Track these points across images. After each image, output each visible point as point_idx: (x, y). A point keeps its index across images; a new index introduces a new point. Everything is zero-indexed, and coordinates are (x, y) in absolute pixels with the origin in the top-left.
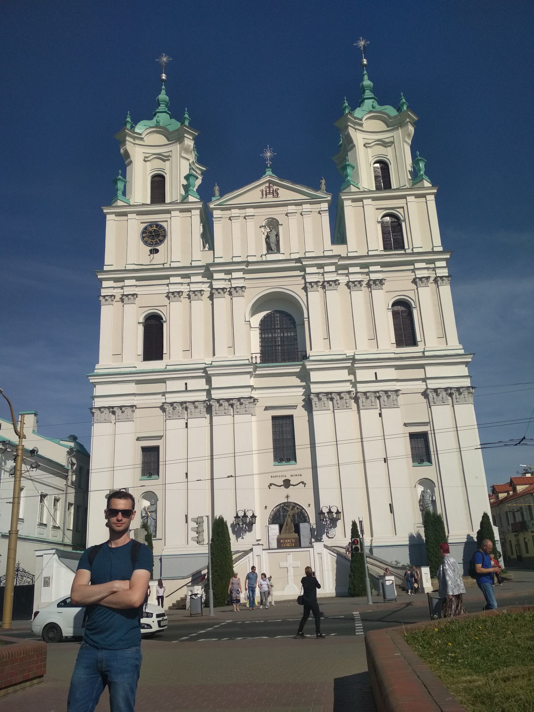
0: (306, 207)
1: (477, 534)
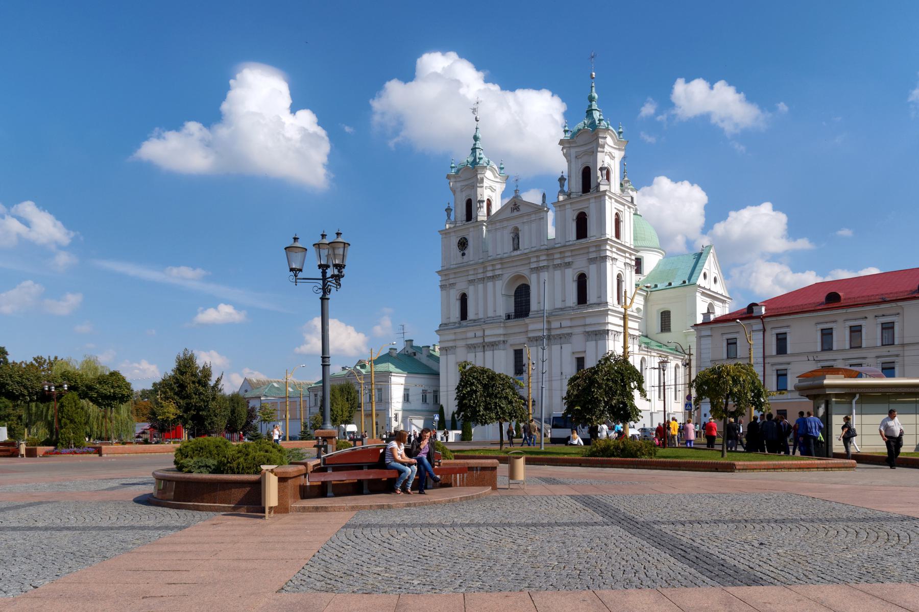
0: (533, 217)
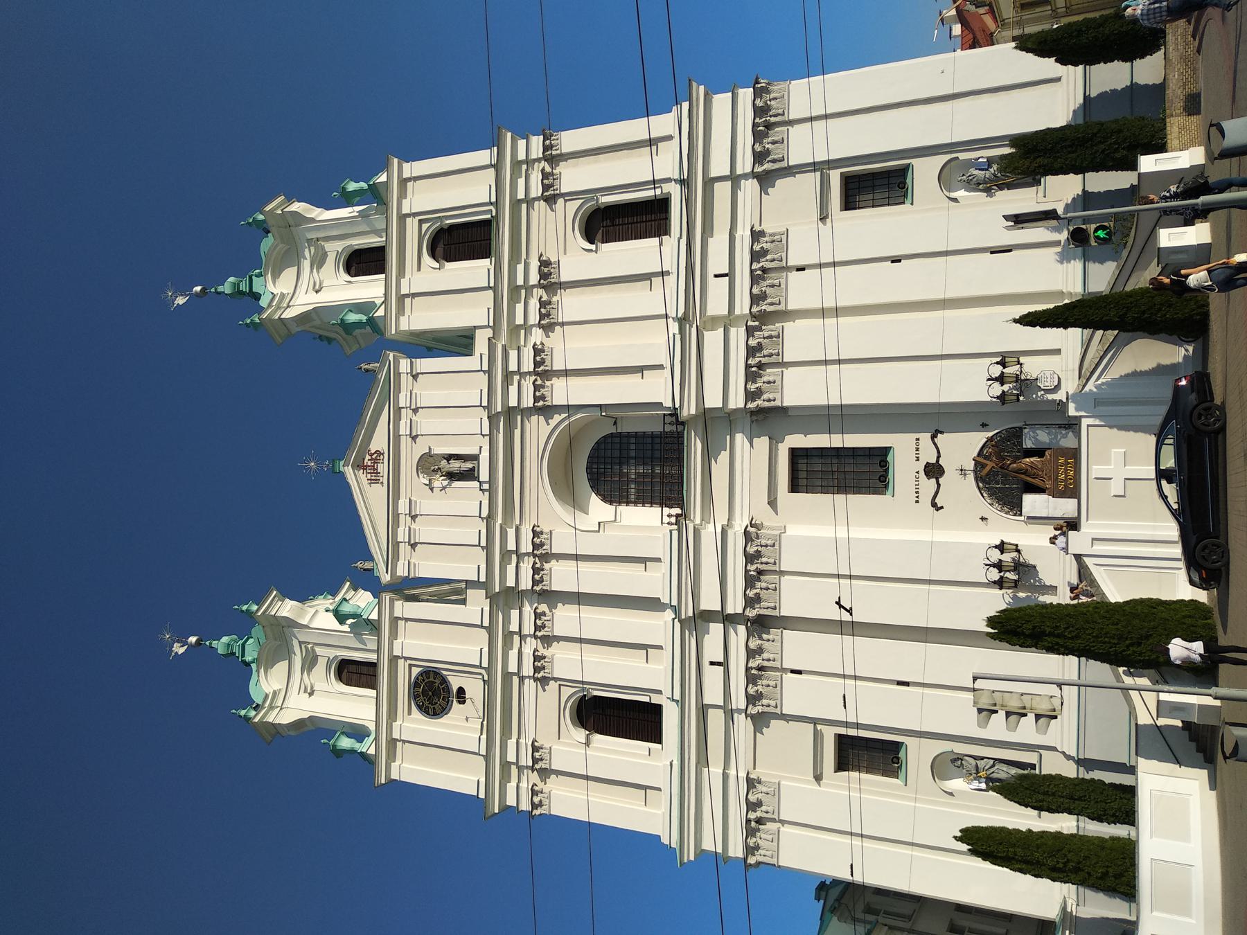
1: (1066, 65)
